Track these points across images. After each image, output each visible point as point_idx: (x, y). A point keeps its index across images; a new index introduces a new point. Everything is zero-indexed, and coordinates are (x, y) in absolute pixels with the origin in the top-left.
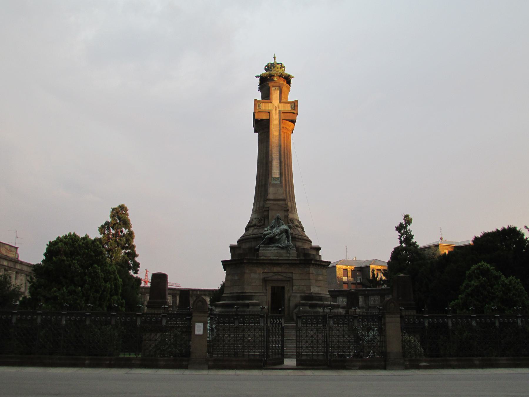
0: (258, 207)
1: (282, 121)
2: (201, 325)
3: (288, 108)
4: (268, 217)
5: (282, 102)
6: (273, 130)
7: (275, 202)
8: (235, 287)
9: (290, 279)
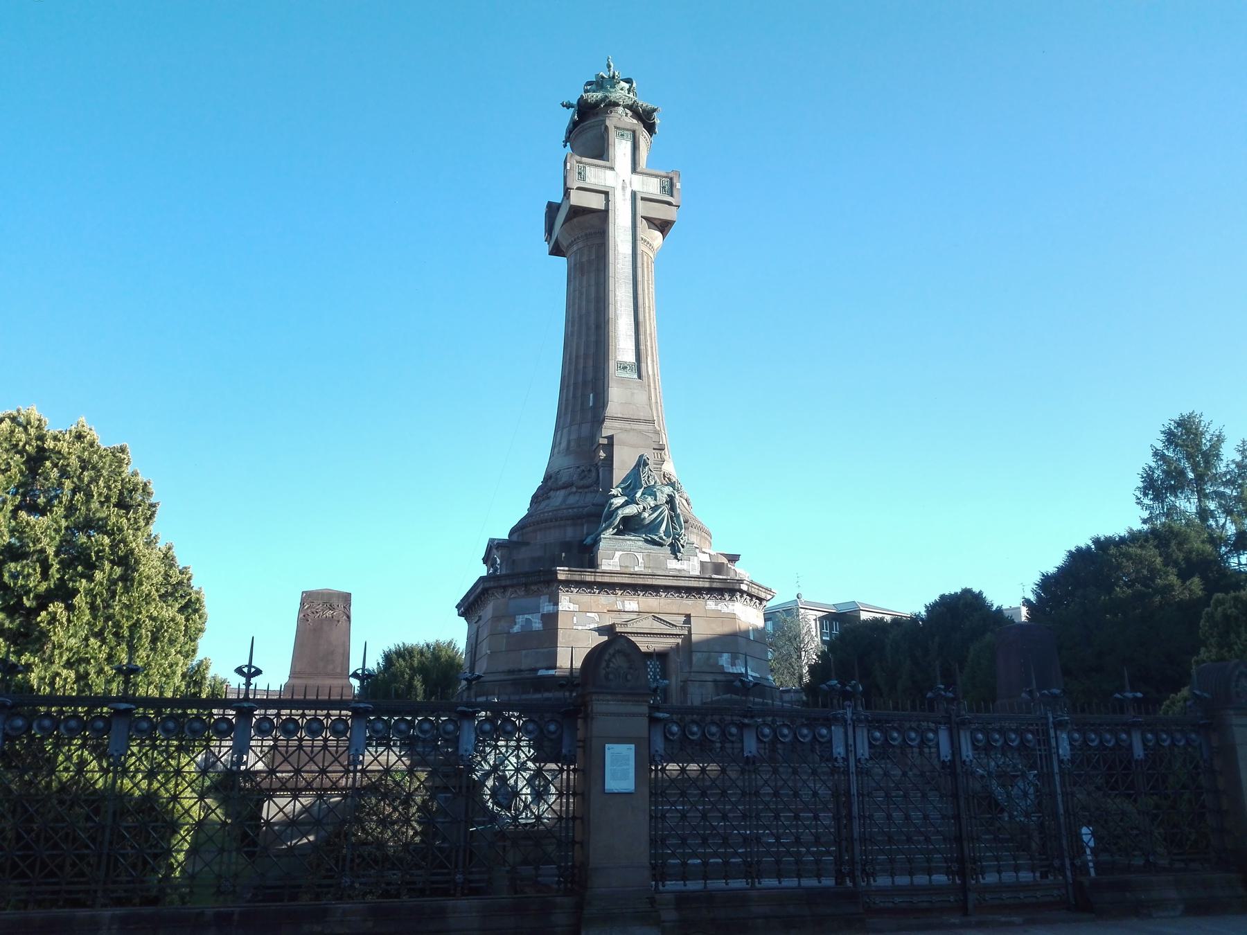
0: (574, 437)
1: (639, 219)
3: (652, 187)
5: (638, 170)
6: (618, 240)
7: (627, 426)
8: (524, 652)
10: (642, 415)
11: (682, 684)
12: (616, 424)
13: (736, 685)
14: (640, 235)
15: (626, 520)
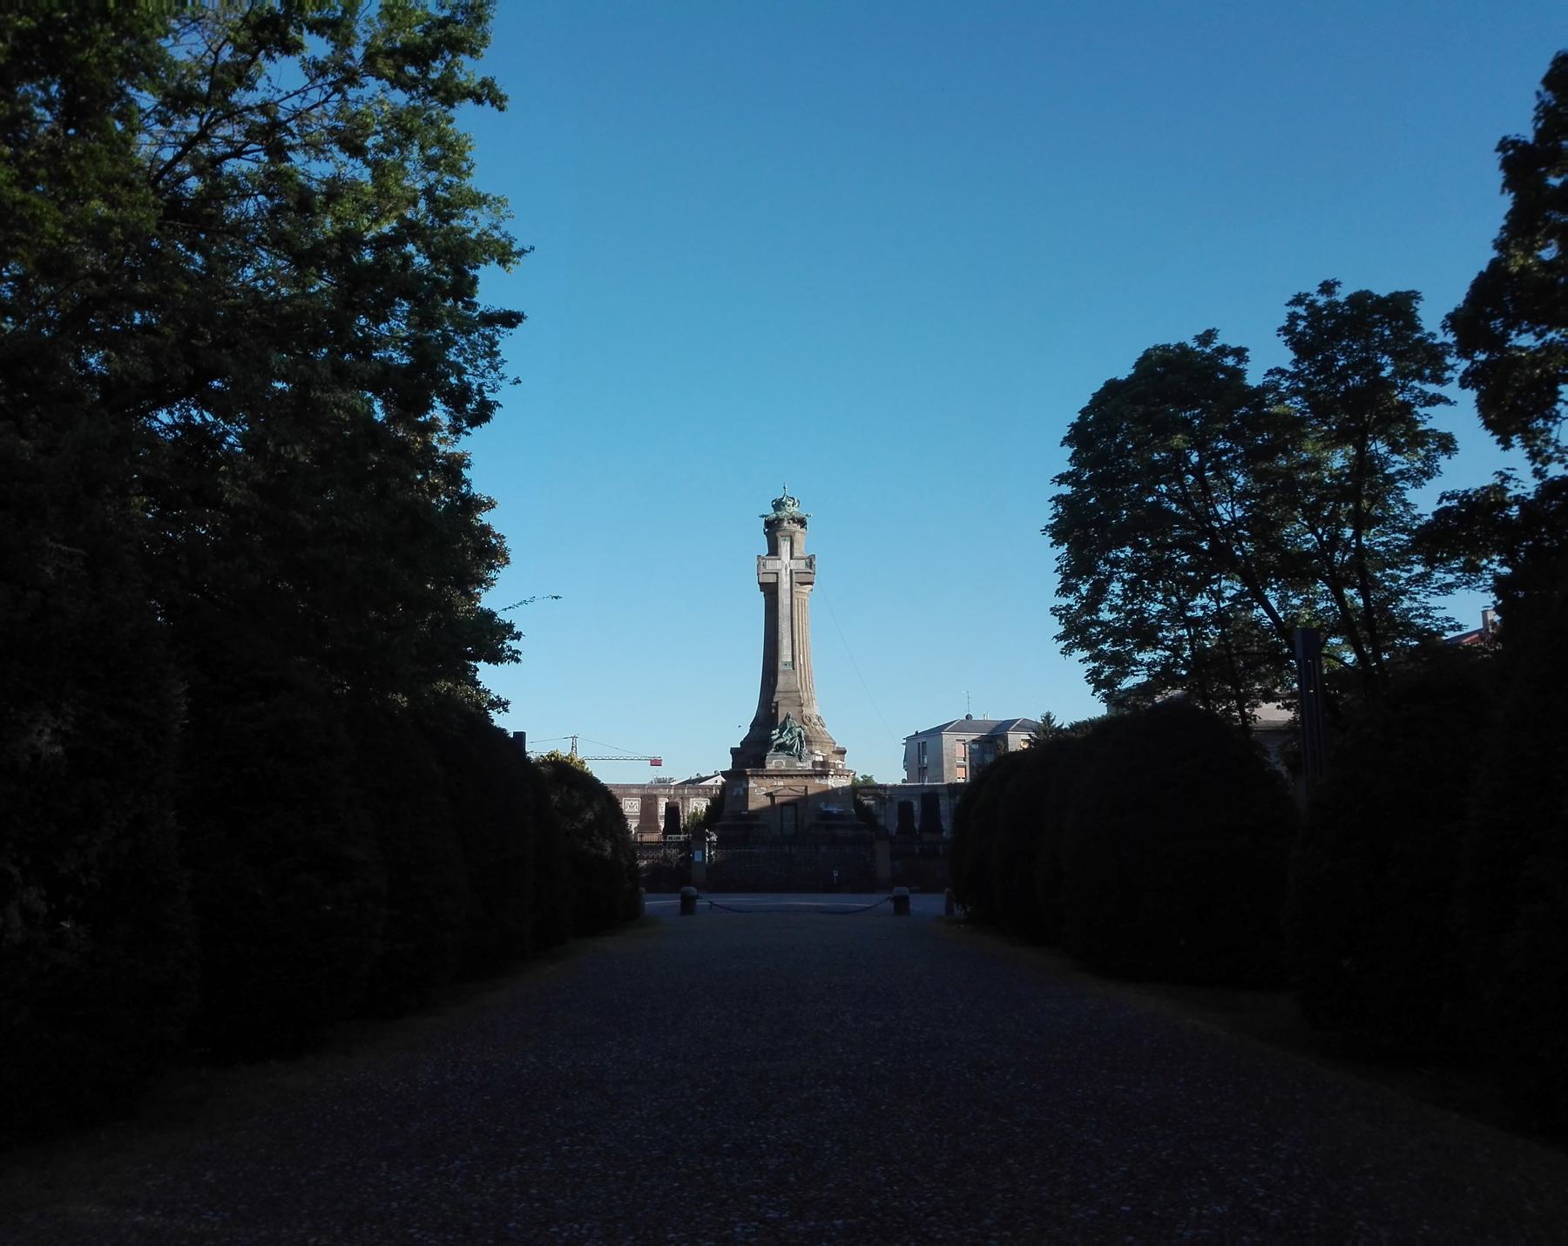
1: (794, 584)
2: (700, 852)
3: (802, 565)
6: (784, 597)
7: (786, 695)
10: (794, 689)
12: (781, 695)
13: (828, 815)
14: (795, 590)
15: (778, 745)
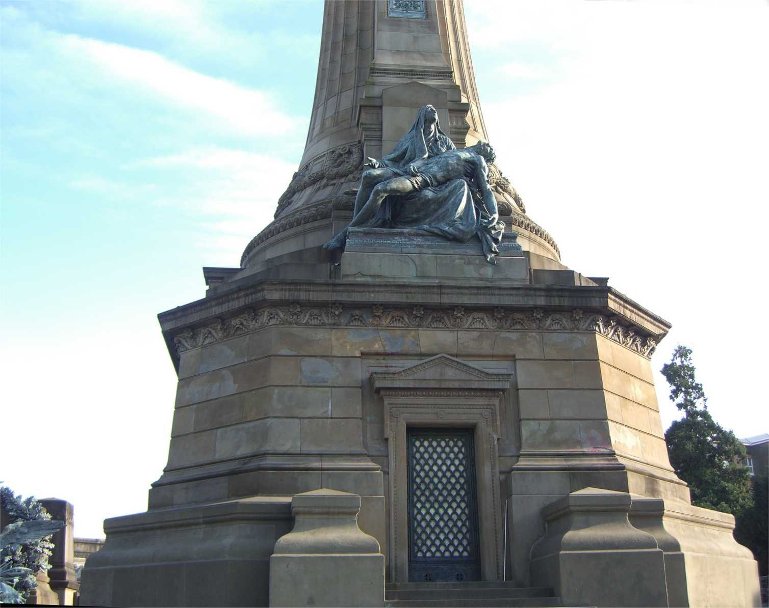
0: (329, 114)
4: (381, 136)
9: (507, 385)
11: (503, 477)
